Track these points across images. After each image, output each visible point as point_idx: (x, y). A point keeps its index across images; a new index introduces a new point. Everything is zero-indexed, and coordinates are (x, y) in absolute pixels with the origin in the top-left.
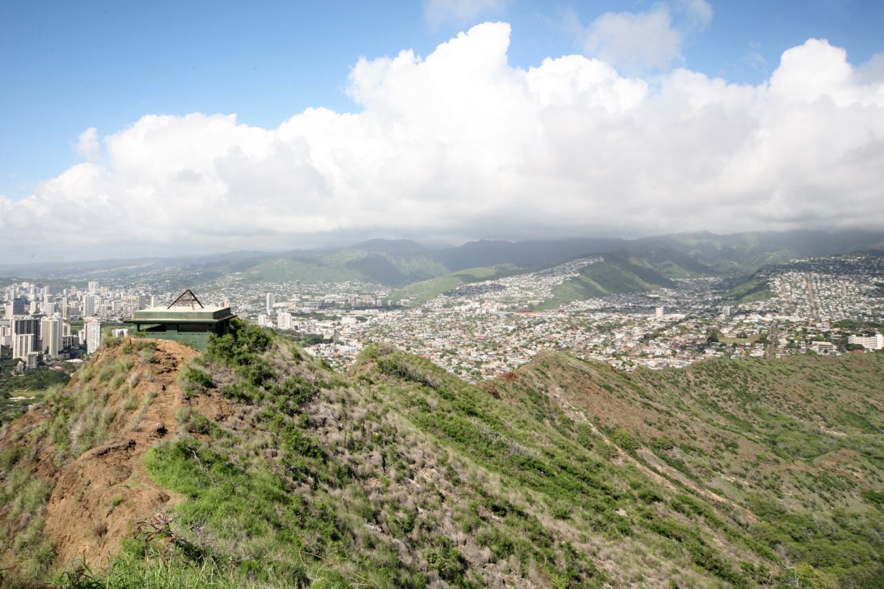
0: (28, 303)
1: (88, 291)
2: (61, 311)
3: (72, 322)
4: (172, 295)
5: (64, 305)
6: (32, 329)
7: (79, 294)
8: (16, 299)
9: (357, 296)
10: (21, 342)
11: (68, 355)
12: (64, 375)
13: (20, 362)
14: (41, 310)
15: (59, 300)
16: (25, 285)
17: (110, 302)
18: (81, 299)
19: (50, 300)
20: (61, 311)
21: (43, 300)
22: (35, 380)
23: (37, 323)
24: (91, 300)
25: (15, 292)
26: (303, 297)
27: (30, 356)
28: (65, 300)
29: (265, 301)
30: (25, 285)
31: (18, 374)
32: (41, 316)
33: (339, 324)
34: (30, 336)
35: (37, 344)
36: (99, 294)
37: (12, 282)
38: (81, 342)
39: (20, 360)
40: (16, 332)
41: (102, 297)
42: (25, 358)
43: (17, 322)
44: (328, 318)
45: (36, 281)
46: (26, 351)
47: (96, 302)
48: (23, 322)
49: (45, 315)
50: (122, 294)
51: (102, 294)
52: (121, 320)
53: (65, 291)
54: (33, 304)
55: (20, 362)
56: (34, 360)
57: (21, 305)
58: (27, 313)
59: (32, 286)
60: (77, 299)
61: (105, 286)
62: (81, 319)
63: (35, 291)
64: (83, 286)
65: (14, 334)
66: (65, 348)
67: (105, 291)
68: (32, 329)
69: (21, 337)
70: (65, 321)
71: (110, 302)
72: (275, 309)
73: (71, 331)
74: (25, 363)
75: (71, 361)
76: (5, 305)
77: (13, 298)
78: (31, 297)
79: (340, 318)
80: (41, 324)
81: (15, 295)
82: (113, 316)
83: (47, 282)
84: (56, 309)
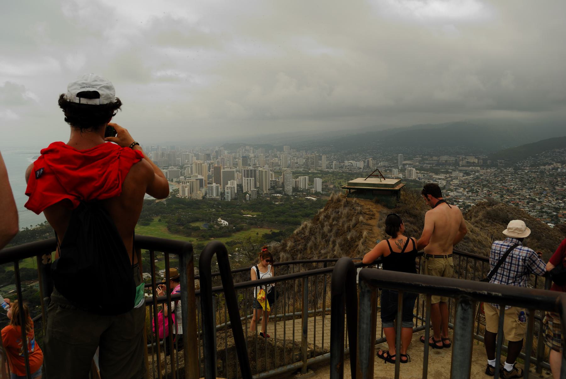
4: (335, 155)
9: (464, 157)
10: (248, 184)
11: (273, 191)
26: (424, 157)
27: (252, 191)
29: (397, 160)
30: (247, 147)
33: (450, 177)
42: (250, 192)
44: (443, 172)
48: (248, 171)
58: (250, 166)
63: (253, 153)
66: (272, 187)
72: (404, 165)
79: (451, 173)
80: (257, 172)
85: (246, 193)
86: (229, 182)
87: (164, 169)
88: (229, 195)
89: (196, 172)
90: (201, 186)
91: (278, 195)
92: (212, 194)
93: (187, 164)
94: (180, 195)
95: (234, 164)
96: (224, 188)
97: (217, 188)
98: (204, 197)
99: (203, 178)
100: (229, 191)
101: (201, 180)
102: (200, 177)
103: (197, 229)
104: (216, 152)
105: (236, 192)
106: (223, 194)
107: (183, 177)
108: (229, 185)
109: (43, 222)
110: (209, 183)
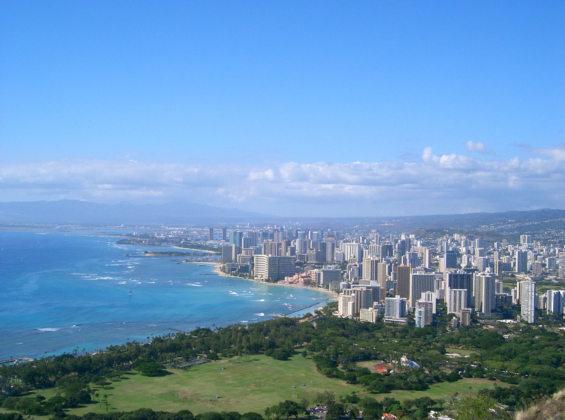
0: (460, 256)
1: (520, 245)
2: (492, 265)
3: (505, 278)
5: (496, 261)
6: (465, 284)
7: (510, 248)
8: (448, 252)
12: (498, 335)
13: (454, 318)
14: (473, 264)
15: (490, 254)
16: (456, 236)
17: (544, 258)
18: (513, 255)
19: (482, 254)
20: (492, 265)
21: (474, 254)
22: (469, 338)
23: (469, 278)
24: (523, 257)
25: (447, 243)
28: (496, 254)
31: (452, 329)
32: (473, 271)
34: (464, 291)
35: (470, 302)
36: (531, 249)
37: (443, 234)
38: (514, 302)
39: (455, 316)
40: (450, 285)
41: (535, 252)
43: (450, 275)
45: (467, 233)
46: (460, 306)
47: (529, 257)
49: (478, 270)
50: (556, 249)
51: (536, 249)
52: (555, 279)
53: (496, 244)
54: (465, 257)
55: (454, 318)
56: (468, 315)
57: (453, 259)
59: (463, 237)
60: (509, 254)
61: (538, 240)
62: (513, 276)
63: (466, 245)
64: (515, 240)
65: (448, 289)
67: (538, 246)
68: (465, 284)
69: (455, 292)
70: (497, 278)
71: (544, 258)
73: (504, 289)
74: (459, 319)
75: (504, 321)
76: (438, 257)
77: (445, 250)
78: (463, 250)
81: (448, 247)
82: (547, 274)
83: (478, 234)
84: (487, 263)
85: (452, 315)
86: (423, 295)
87: (314, 268)
88: (423, 316)
89: (368, 276)
91: (508, 321)
93: (352, 261)
94: (340, 313)
95: (430, 264)
97: (403, 304)
100: (423, 310)
101: (376, 289)
102: (373, 284)
103: (366, 372)
104: (403, 242)
105: (434, 312)
106: (411, 316)
108: (422, 300)
109: (125, 344)
110: (388, 295)
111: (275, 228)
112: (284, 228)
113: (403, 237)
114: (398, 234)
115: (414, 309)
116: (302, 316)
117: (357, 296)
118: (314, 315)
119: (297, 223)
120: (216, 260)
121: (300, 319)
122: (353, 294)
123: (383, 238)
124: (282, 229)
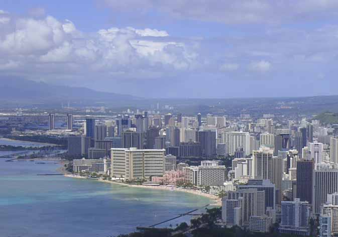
87: (190, 164)
90: (269, 203)
92: (292, 222)
96: (318, 209)
98: (274, 229)
99: (273, 186)
104: (303, 130)
107: (231, 183)
111: (138, 113)
112: (149, 112)
113: (304, 123)
114: (297, 119)
115: (318, 215)
116: (174, 227)
117: (246, 201)
118: (189, 224)
119: (167, 107)
120: (59, 155)
121: (172, 230)
122: (240, 198)
123: (278, 125)
124: (146, 113)
